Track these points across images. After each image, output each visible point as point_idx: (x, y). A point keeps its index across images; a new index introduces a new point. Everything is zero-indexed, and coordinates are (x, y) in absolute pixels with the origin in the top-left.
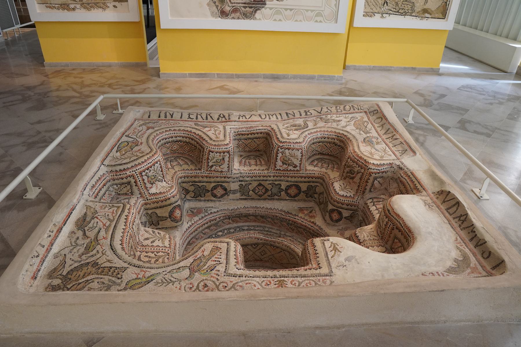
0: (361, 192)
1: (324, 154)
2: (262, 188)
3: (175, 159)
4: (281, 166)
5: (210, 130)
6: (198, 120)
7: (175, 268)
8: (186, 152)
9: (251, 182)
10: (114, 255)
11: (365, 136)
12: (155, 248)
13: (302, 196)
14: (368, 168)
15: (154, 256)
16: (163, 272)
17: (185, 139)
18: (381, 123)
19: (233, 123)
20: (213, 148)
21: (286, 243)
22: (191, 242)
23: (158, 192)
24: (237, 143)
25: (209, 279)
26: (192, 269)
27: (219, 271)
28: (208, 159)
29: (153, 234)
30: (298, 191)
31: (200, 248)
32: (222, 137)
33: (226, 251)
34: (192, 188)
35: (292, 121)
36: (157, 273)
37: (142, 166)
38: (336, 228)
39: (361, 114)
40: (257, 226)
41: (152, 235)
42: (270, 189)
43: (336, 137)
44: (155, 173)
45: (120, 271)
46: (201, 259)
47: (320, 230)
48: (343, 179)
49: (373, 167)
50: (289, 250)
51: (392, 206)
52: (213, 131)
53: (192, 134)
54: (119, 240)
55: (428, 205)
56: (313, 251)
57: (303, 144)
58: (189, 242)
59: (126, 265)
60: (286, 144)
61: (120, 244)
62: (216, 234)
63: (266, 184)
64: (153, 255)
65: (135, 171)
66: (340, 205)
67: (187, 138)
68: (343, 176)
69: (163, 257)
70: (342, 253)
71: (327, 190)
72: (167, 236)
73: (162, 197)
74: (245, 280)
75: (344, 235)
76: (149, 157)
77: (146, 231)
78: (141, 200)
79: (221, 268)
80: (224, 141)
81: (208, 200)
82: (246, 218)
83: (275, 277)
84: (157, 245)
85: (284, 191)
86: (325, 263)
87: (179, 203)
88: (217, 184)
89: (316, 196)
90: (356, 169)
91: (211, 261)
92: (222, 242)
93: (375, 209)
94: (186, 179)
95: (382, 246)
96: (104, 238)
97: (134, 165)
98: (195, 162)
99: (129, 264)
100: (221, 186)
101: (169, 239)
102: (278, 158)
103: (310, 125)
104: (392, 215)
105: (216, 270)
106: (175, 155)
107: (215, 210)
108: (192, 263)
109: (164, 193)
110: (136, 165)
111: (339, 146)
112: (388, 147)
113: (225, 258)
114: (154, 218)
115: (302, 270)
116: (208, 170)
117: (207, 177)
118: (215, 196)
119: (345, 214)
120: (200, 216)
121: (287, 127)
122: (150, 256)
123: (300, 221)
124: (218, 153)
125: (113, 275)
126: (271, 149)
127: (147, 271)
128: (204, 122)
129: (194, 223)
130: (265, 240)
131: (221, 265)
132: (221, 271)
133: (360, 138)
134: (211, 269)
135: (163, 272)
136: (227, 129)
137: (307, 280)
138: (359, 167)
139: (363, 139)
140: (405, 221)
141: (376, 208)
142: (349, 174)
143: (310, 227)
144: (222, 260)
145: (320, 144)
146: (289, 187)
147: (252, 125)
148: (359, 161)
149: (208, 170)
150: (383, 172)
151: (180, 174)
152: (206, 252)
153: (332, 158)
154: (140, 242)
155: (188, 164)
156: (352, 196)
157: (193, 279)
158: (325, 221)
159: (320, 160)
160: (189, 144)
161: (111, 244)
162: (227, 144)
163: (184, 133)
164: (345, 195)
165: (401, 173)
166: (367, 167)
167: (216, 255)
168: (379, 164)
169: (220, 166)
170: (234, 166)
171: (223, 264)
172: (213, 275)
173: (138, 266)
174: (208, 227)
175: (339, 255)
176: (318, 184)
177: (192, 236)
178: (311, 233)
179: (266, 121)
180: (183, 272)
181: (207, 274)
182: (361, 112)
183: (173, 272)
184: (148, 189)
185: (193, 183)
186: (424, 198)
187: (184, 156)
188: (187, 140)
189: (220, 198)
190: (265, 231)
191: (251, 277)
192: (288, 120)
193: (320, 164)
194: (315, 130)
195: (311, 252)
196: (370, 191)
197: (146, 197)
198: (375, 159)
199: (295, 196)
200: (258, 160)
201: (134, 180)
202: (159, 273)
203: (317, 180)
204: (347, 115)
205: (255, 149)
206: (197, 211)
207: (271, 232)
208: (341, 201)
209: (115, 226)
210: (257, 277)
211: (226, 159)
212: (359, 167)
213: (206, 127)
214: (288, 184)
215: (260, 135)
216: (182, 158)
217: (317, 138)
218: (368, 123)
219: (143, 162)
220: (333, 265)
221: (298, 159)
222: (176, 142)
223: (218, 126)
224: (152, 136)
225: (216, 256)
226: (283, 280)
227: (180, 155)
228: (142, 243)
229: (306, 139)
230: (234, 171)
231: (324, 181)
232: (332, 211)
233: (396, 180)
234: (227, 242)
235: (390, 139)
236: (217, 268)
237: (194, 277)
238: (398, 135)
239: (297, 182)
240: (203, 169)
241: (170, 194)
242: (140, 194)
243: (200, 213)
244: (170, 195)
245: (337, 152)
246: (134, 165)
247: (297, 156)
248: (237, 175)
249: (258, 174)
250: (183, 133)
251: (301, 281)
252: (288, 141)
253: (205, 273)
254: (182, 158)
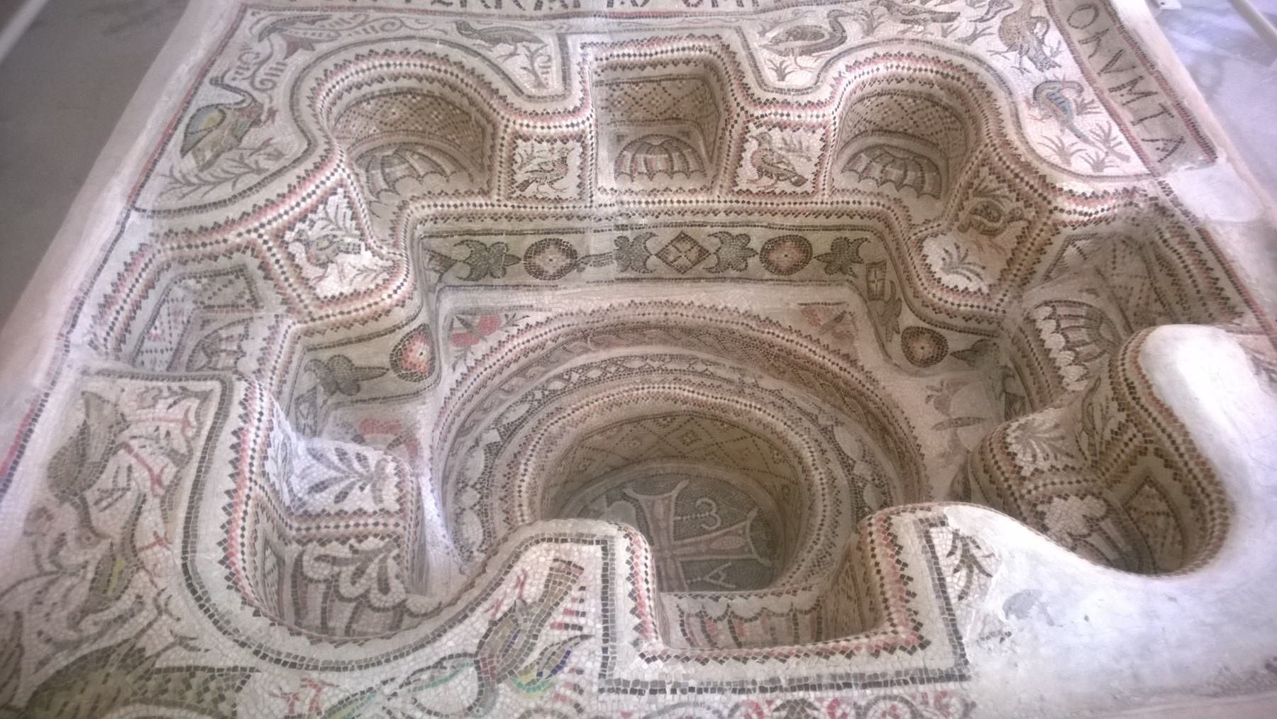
0: (1018, 279)
1: (890, 132)
2: (688, 246)
3: (396, 152)
4: (753, 182)
5: (512, 55)
6: (468, 9)
7: (424, 665)
8: (435, 128)
9: (654, 231)
10: (200, 613)
11: (1037, 76)
12: (352, 523)
13: (814, 266)
14: (1051, 207)
15: (350, 555)
16: (385, 683)
17: (426, 86)
18: (1093, 29)
19: (591, 22)
20: (528, 126)
21: (759, 414)
22: (467, 425)
23: (347, 290)
24: (605, 96)
25: (548, 706)
26: (485, 666)
27: (580, 672)
28: (511, 160)
29: (340, 465)
30: (802, 256)
31: (510, 567)
32: (555, 84)
33: (599, 582)
34: (462, 253)
35: (790, 16)
36: (363, 693)
37: (282, 211)
38: (924, 382)
40: (672, 357)
41: (336, 469)
42: (712, 250)
43: (939, 76)
44: (331, 227)
45: (228, 688)
46: (516, 621)
47: (868, 385)
48: (954, 228)
49: (1069, 205)
50: (769, 436)
51: (1144, 372)
52: (522, 59)
53: (449, 69)
54: (213, 544)
55: (1267, 370)
56: (894, 567)
57: (828, 110)
58: (463, 425)
59: (243, 658)
60: (773, 111)
61: (222, 562)
62: (544, 389)
63: (701, 235)
64: (343, 551)
65: (256, 230)
66: (942, 317)
67: (436, 84)
68: (957, 220)
69: (381, 556)
70: (993, 580)
71: (898, 262)
72: (390, 468)
73: (360, 308)
74: (675, 707)
75: (948, 408)
76: (303, 174)
77: (314, 457)
78: (290, 322)
79: (587, 658)
80: (564, 97)
81: (517, 287)
82: (636, 335)
83: (773, 685)
84: (356, 508)
85: (757, 257)
86: (941, 625)
87: (423, 318)
88: (543, 237)
89: (858, 269)
90: (1008, 206)
91: (552, 626)
92: (585, 542)
93: (1063, 344)
94: (438, 226)
95: (1093, 494)
96: (159, 541)
97: (250, 209)
98: (466, 163)
99: (256, 653)
100: (558, 243)
101: (396, 479)
102: (747, 155)
103: (854, 32)
104: (1142, 407)
105: (572, 670)
106: (401, 138)
107: (540, 317)
108: (486, 636)
109: (369, 292)
110: (258, 210)
111: (946, 109)
112: (1119, 125)
113: (600, 611)
114: (342, 371)
115: (863, 650)
116: (514, 196)
117: (509, 217)
118: (538, 273)
119: (956, 342)
120: (492, 341)
121: (776, 41)
122: (335, 558)
123: (804, 351)
124: (545, 144)
125: (204, 705)
126: (722, 124)
127: (324, 683)
128: (489, 15)
129: (473, 364)
130: (696, 403)
131: (586, 643)
132: (587, 672)
133: (1022, 87)
134: (554, 666)
135: (385, 683)
136: (571, 50)
137: (884, 698)
138: (1018, 200)
139: (1031, 91)
140: (1191, 437)
141: (1068, 342)
142: (979, 218)
143: (836, 369)
144: (591, 623)
145: (884, 99)
146: (774, 244)
147: (654, 34)
148: (1022, 179)
149: (514, 196)
150: (1100, 220)
151: (419, 210)
152: (531, 584)
153: (916, 147)
154: (297, 503)
155: (442, 173)
156: (985, 290)
157: (494, 712)
158: (888, 356)
159: (878, 152)
160: (443, 105)
161: (184, 566)
162: (576, 111)
163: (422, 66)
164: (961, 288)
165: (1163, 228)
166: (1049, 203)
167: (568, 598)
168: (1088, 195)
169: (551, 183)
170: (600, 177)
171: (592, 640)
172: (562, 691)
173: (290, 660)
174: (522, 372)
175: (984, 590)
176: (868, 235)
177: (469, 407)
178: (838, 389)
179: (702, 14)
180: (456, 680)
181: (539, 688)
183: (419, 684)
184: (311, 283)
185: (466, 237)
186: (1250, 338)
187: (427, 141)
188: (436, 88)
189: (553, 277)
190: (694, 373)
191: (692, 689)
192: (777, 9)
193: (876, 172)
194: (869, 53)
195: (884, 567)
196: (1047, 277)
197: (306, 311)
198: (1077, 175)
199: (790, 271)
200: (675, 155)
201: (257, 262)
202: (370, 689)
203: (866, 222)
205: (667, 115)
206: (482, 324)
207: (712, 376)
208: (948, 305)
209: (197, 486)
210: (713, 691)
211: (574, 161)
212: (1018, 200)
213: (496, 41)
214: (771, 234)
215: (683, 69)
216: (421, 150)
217: (874, 81)
218: (1048, 26)
219: (283, 196)
220: (968, 635)
221: (809, 159)
222: (395, 94)
223: (539, 34)
224: (309, 83)
225: (567, 604)
226: (803, 701)
227: (413, 139)
228: (304, 504)
229: (841, 89)
230: (600, 198)
231: (889, 226)
232: (915, 333)
233: (1140, 248)
234: (604, 542)
235: (1124, 91)
236: (573, 661)
237: (494, 703)
238: (1152, 79)
239: (800, 228)
240: (496, 191)
241: (390, 296)
242: (284, 302)
243: (491, 330)
244: (388, 301)
245: (937, 128)
246: (250, 209)
247: (808, 148)
248: (610, 210)
249: (676, 205)
250: (418, 63)
251: (863, 703)
252: (780, 97)
253: (533, 682)
254: (421, 150)
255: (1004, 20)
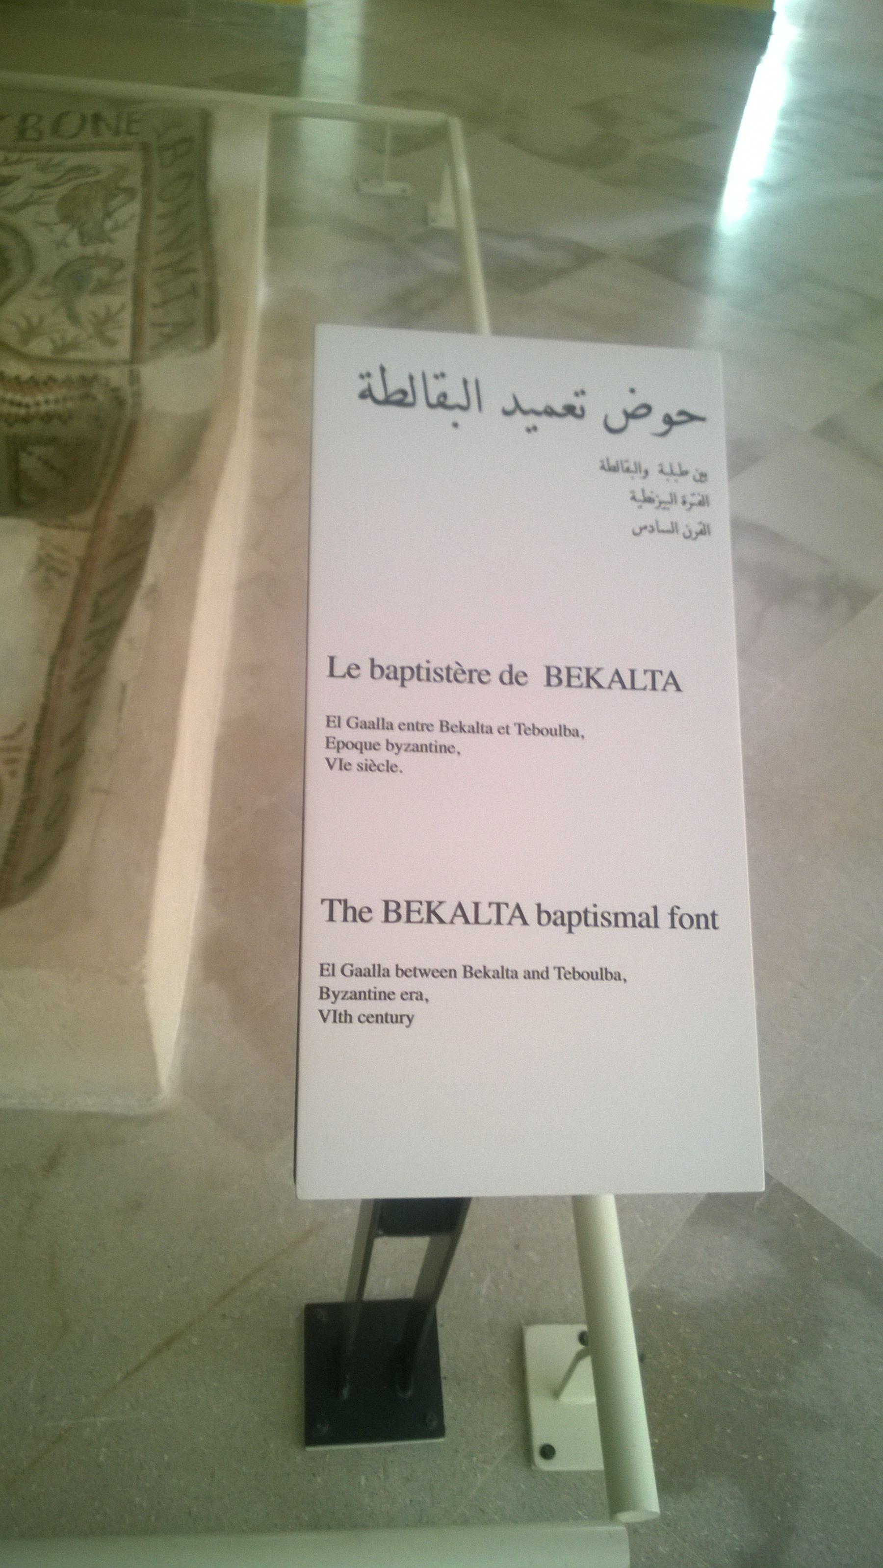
39: (122, 157)
182: (123, 148)
204: (57, 157)
255: (75, 189)
